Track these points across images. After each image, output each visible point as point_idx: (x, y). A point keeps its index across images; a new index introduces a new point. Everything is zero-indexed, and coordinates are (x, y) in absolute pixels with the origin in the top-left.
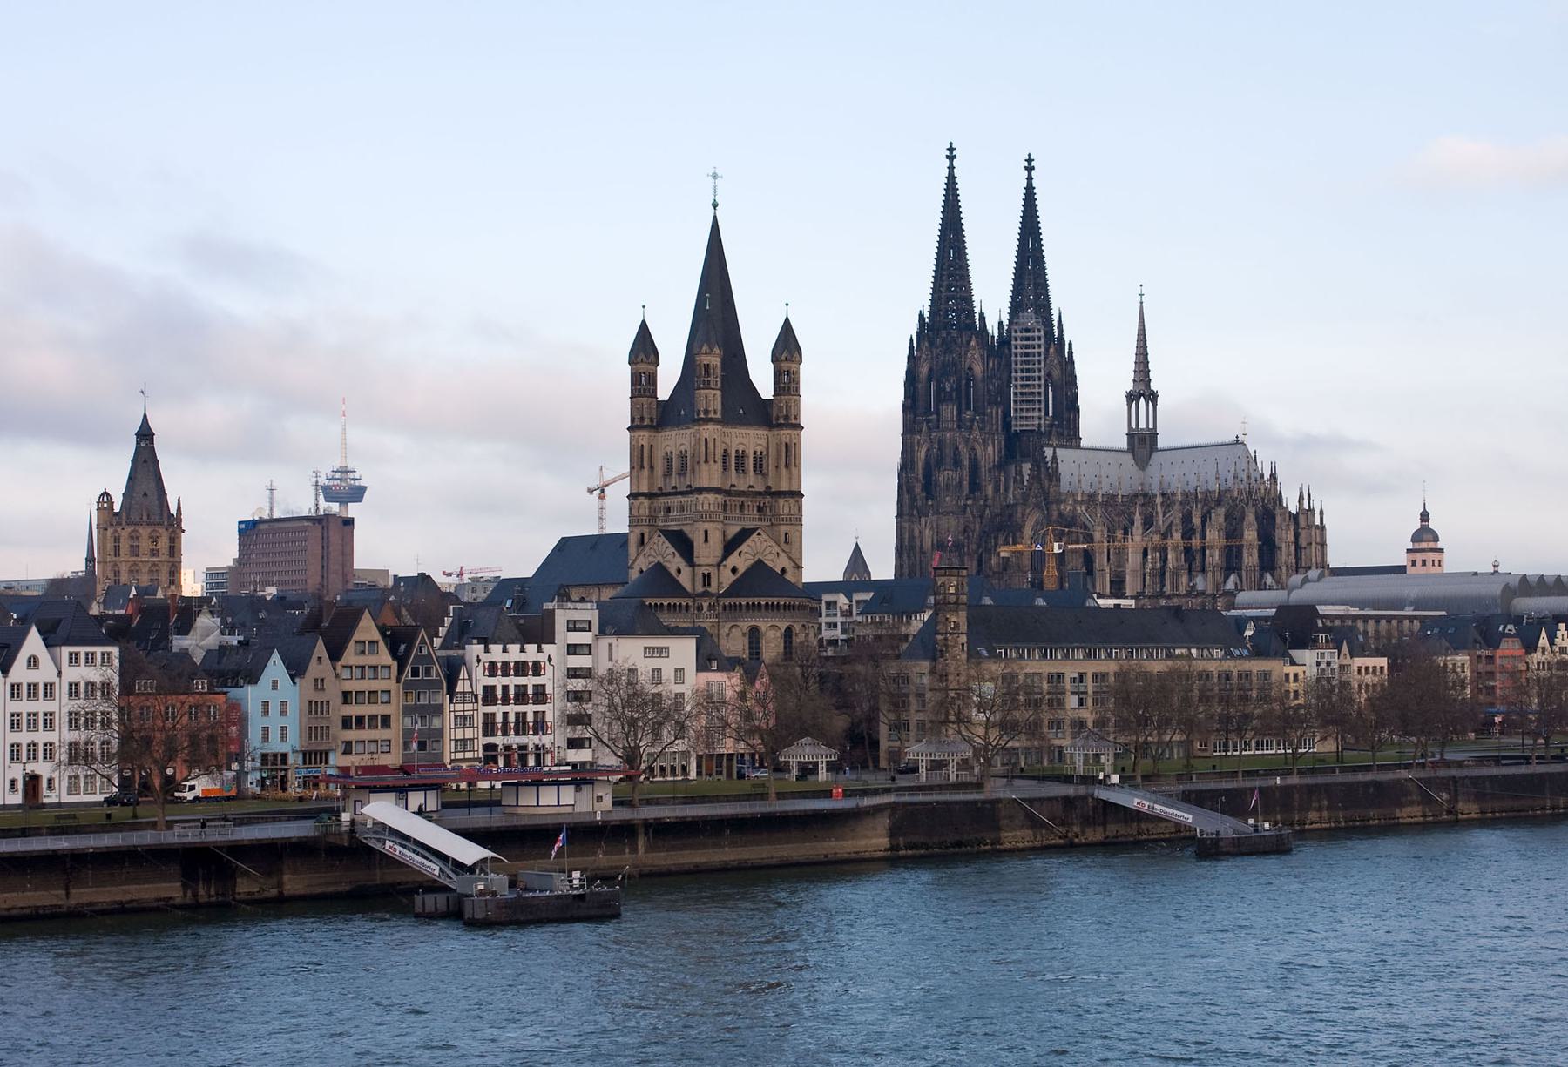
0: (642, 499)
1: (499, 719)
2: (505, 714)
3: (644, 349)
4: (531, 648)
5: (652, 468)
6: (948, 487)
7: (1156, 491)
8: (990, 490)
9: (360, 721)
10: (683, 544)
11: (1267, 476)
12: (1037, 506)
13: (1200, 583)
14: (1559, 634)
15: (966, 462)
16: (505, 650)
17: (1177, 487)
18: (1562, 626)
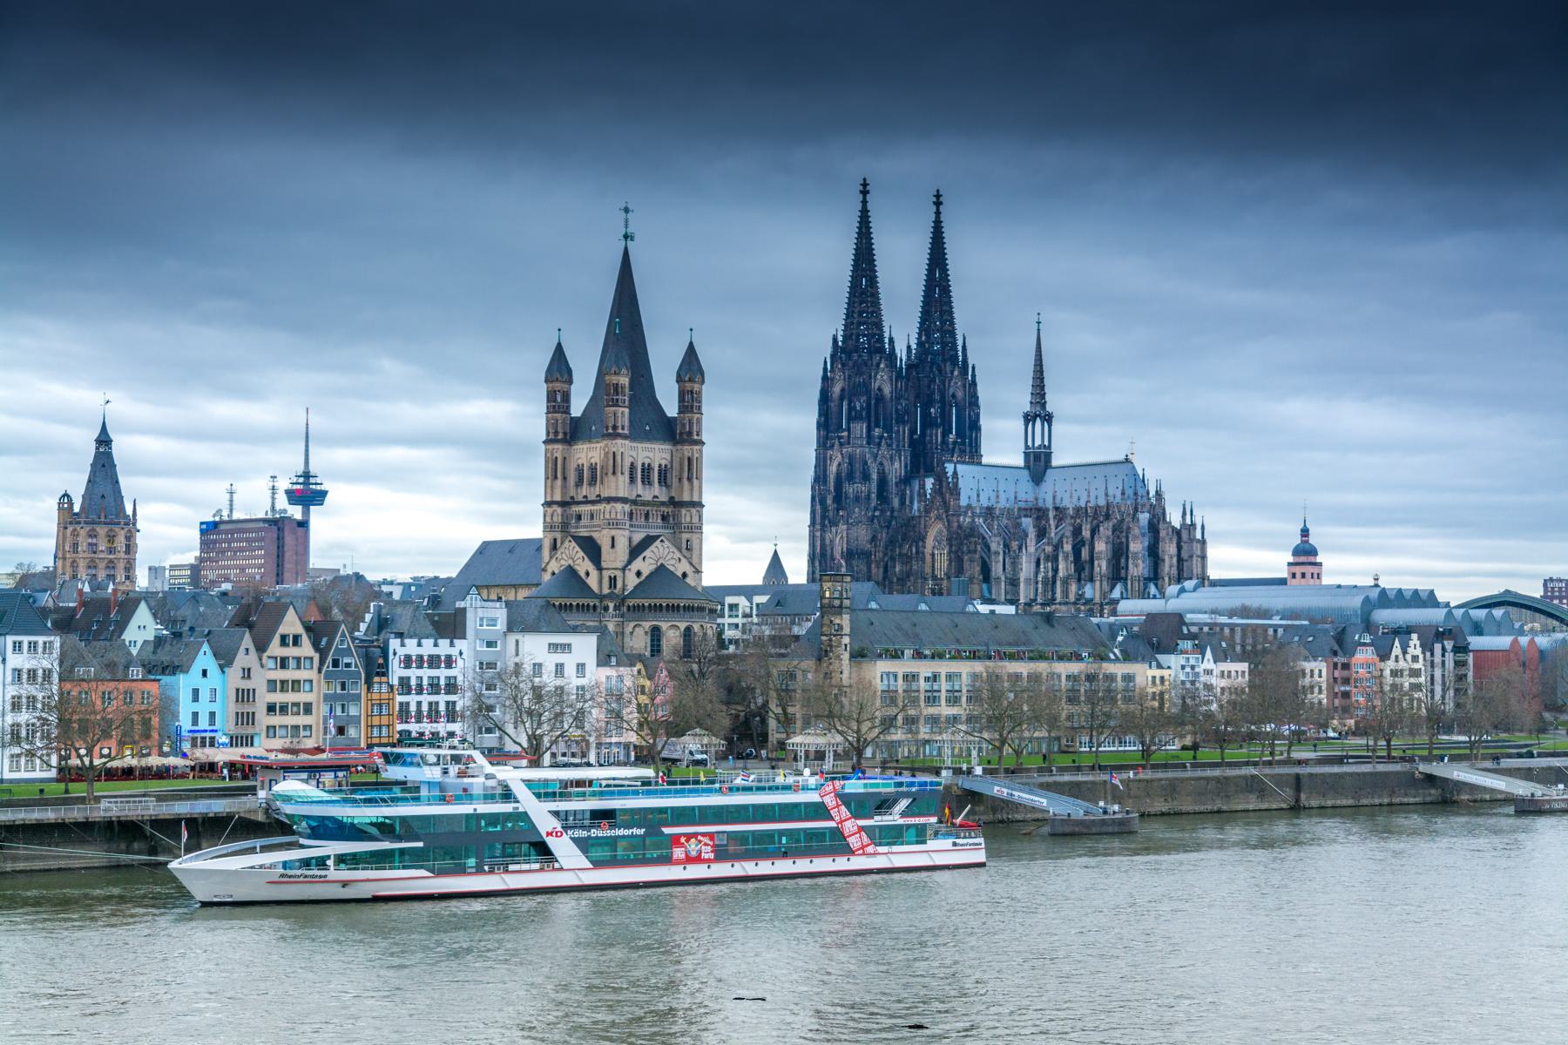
0: (555, 507)
1: (413, 708)
2: (419, 704)
3: (559, 370)
4: (444, 643)
5: (565, 478)
6: (857, 499)
7: (1050, 505)
8: (896, 502)
9: (284, 709)
10: (592, 549)
11: (1152, 493)
12: (939, 518)
13: (1088, 591)
14: (1411, 643)
15: (875, 476)
16: (419, 645)
17: (1068, 503)
18: (1414, 636)
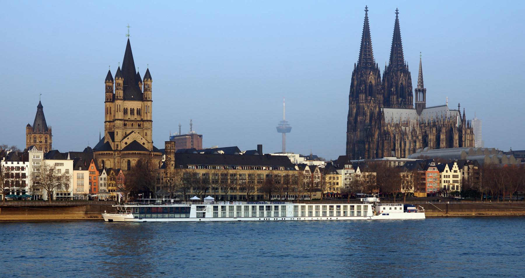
0: (107, 123)
6: (361, 122)
15: (368, 114)
18: (455, 163)
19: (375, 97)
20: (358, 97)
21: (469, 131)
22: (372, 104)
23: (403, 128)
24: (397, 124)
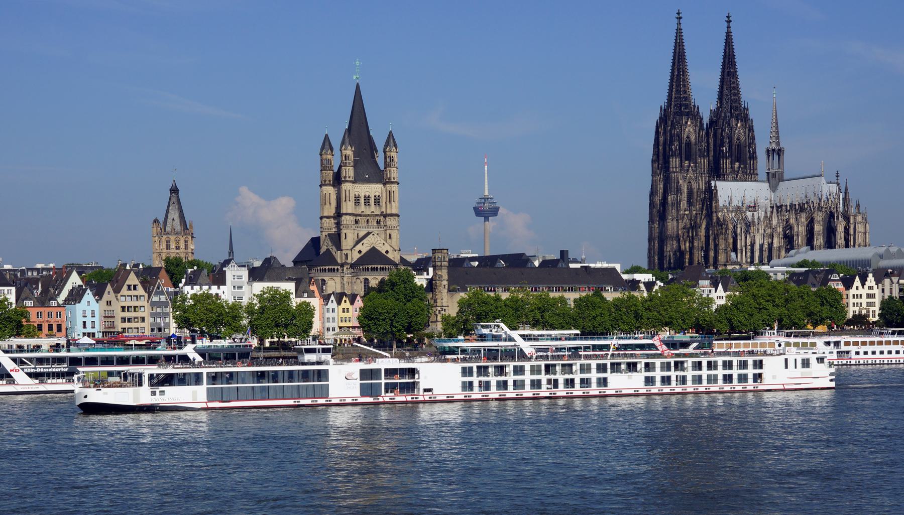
6: (673, 204)
15: (685, 190)
19: (695, 163)
20: (668, 162)
21: (860, 218)
22: (691, 174)
23: (749, 214)
24: (739, 207)
